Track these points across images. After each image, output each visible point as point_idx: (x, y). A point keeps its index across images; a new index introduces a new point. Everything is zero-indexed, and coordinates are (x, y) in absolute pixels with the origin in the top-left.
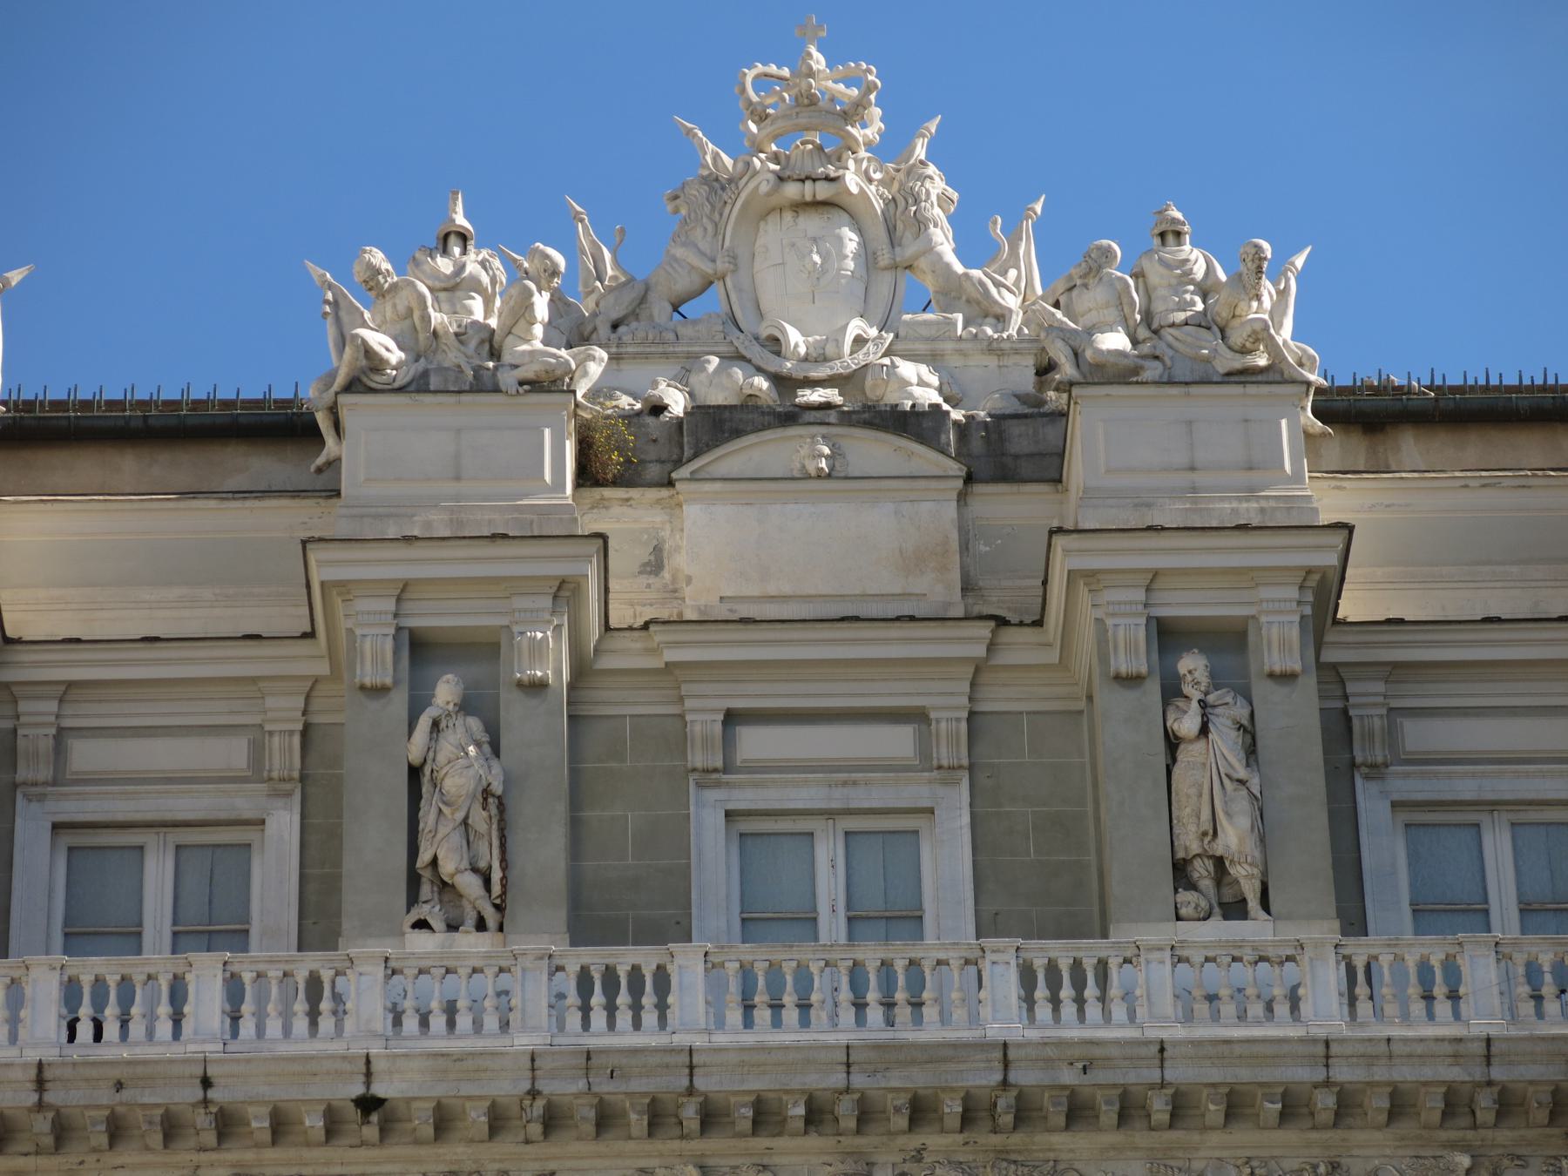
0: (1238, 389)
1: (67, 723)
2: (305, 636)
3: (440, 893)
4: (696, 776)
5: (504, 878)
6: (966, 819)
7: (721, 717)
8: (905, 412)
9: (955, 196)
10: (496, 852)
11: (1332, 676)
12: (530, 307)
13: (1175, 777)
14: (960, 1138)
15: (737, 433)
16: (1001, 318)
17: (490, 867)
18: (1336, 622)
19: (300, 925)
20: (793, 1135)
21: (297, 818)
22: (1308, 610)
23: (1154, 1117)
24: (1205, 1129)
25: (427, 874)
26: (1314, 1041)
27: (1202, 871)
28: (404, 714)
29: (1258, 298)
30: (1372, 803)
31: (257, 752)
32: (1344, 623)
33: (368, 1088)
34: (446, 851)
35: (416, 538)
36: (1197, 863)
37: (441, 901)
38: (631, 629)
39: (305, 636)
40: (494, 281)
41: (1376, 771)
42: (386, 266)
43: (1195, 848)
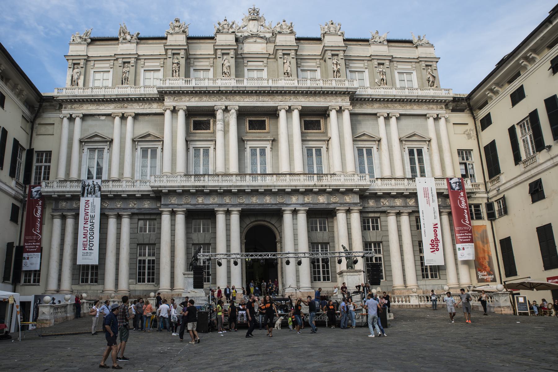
11: (296, 59)
34: (225, 70)
41: (299, 67)
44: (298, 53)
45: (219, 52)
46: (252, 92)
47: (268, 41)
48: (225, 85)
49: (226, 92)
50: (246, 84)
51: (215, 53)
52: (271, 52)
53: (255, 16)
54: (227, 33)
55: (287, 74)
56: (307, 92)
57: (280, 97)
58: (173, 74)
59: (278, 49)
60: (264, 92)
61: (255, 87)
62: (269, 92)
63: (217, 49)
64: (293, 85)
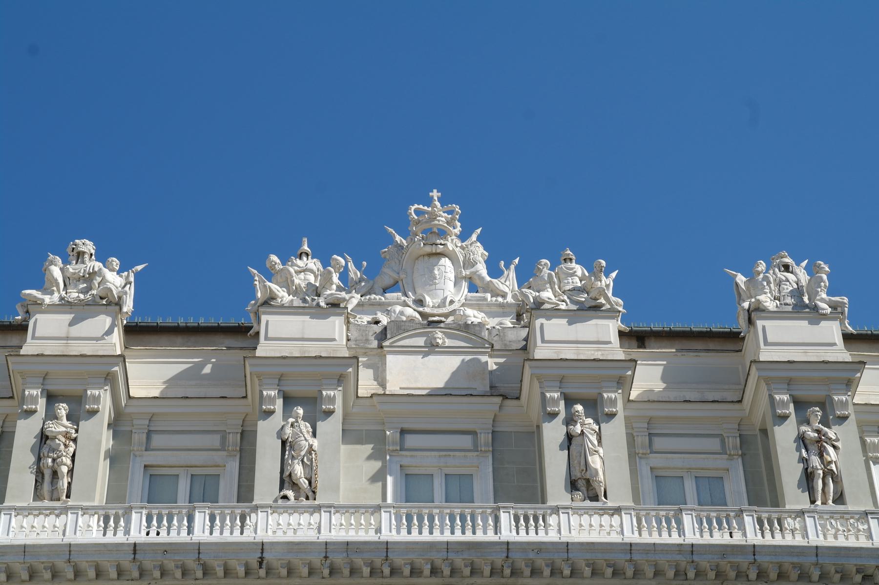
0: (594, 312)
1: (152, 429)
2: (244, 397)
6: (491, 469)
9: (487, 254)
12: (331, 278)
16: (504, 296)
24: (583, 578)
25: (287, 480)
27: (581, 484)
29: (601, 281)
31: (224, 440)
36: (579, 481)
39: (244, 397)
40: (318, 270)
41: (644, 456)
42: (278, 261)
43: (579, 475)
58: (39, 483)
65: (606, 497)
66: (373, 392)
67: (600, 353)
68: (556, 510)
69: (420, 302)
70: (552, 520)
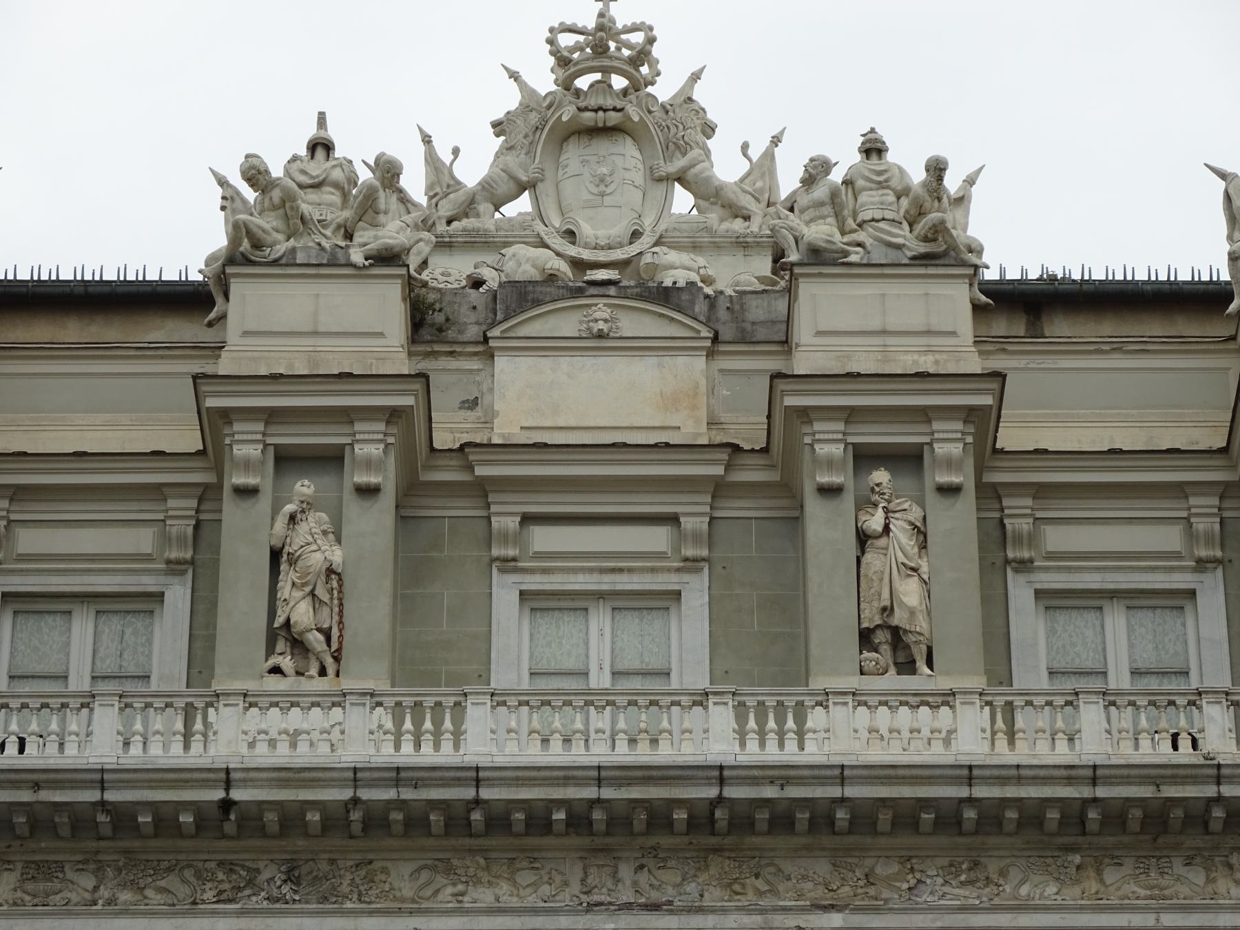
3: (292, 648)
4: (497, 563)
5: (341, 636)
7: (518, 519)
8: (666, 288)
10: (336, 618)
11: (989, 494)
13: (863, 566)
14: (686, 839)
15: (538, 303)
17: (330, 628)
18: (995, 451)
19: (188, 673)
20: (558, 835)
21: (189, 591)
22: (970, 439)
23: (838, 824)
26: (961, 767)
27: (881, 637)
28: (269, 511)
30: (1020, 592)
32: (1002, 451)
33: (228, 794)
35: (281, 375)
37: (292, 654)
38: (450, 450)
39: (198, 453)
41: (1024, 566)
44: (1008, 438)
45: (247, 446)
46: (538, 820)
47: (726, 326)
48: (283, 755)
49: (291, 819)
50: (489, 739)
51: (212, 452)
52: (748, 428)
53: (601, 104)
54: (332, 264)
55: (891, 644)
56: (1075, 817)
57: (822, 868)
59: (805, 414)
60: (659, 817)
61: (567, 775)
62: (702, 819)
63: (226, 415)
64: (936, 754)
65: (930, 663)
66: (466, 438)
67: (930, 358)
68: (824, 699)
69: (570, 235)
70: (816, 718)
